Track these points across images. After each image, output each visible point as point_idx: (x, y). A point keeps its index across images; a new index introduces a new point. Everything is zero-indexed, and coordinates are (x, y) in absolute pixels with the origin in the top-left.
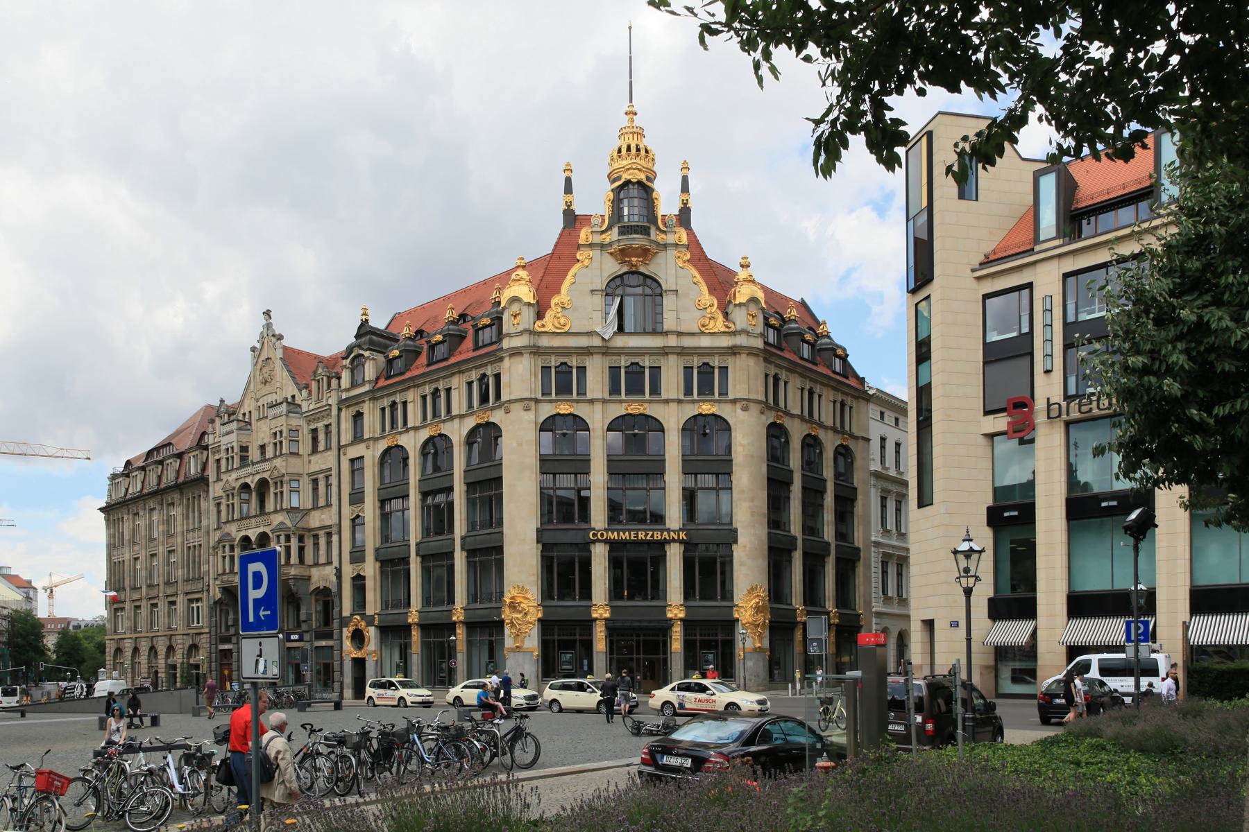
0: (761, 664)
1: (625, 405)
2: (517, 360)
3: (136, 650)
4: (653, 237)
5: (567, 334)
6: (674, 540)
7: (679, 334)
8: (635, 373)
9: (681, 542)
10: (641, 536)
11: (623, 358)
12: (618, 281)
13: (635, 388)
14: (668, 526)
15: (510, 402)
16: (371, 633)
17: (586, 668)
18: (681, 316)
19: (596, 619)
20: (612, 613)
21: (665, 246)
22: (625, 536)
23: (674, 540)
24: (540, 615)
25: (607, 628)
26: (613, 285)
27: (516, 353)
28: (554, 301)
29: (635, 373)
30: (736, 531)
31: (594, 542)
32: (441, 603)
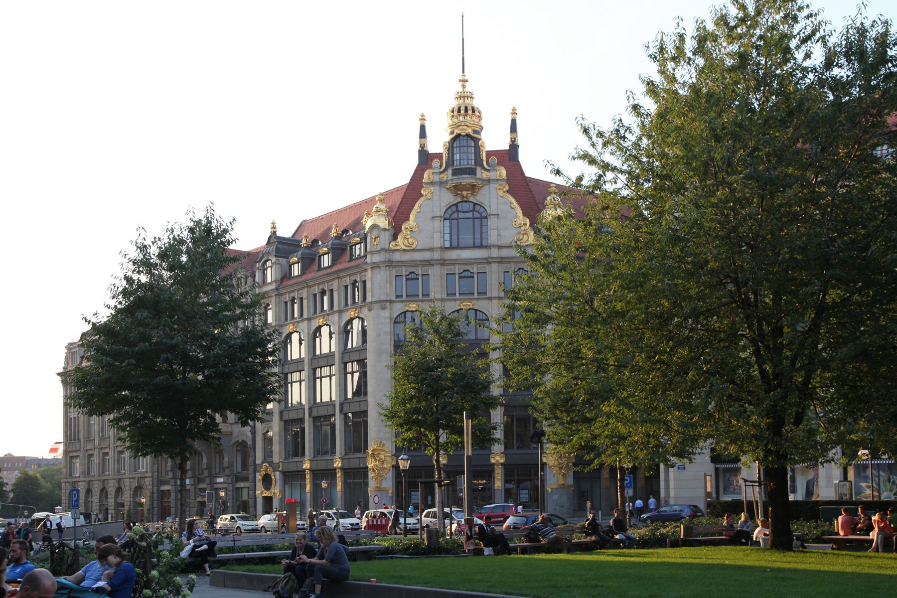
1: (458, 302)
2: (376, 271)
3: (89, 491)
4: (478, 175)
5: (414, 250)
7: (500, 247)
8: (466, 276)
11: (457, 267)
12: (454, 208)
15: (371, 303)
16: (277, 477)
17: (430, 502)
18: (502, 233)
20: (448, 461)
21: (489, 181)
26: (449, 212)
27: (375, 266)
29: (466, 276)
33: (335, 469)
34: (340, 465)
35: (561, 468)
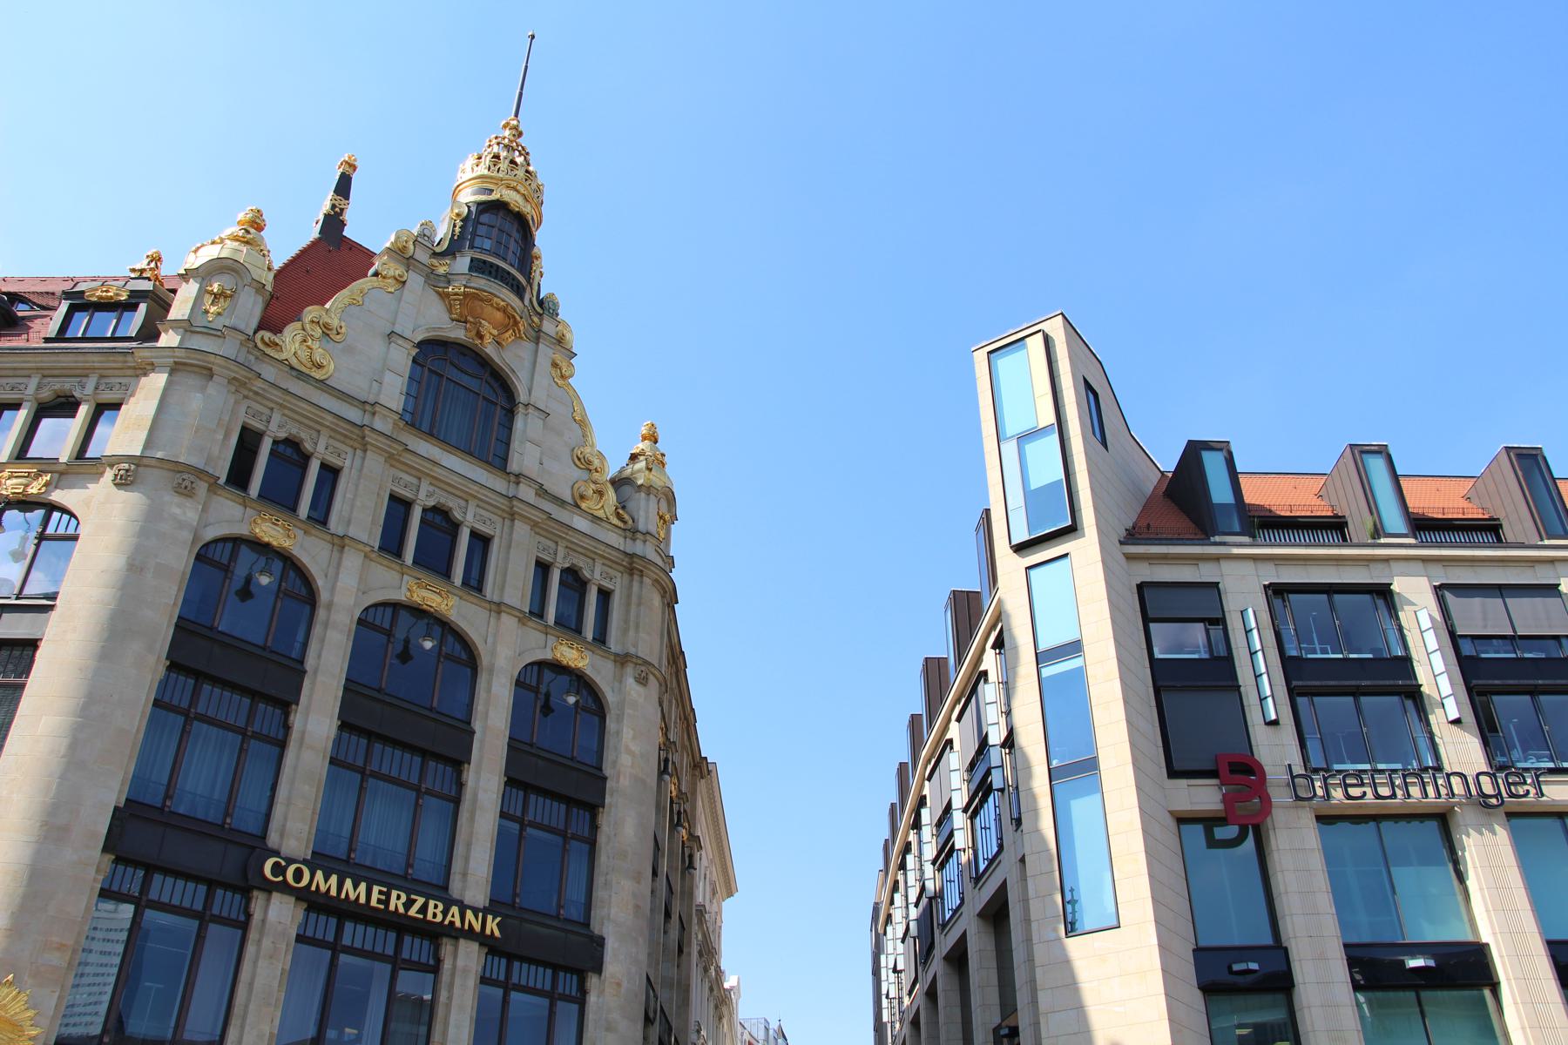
5: (322, 385)
6: (470, 934)
10: (397, 902)
13: (434, 560)
22: (354, 891)
28: (311, 312)
30: (600, 942)
31: (269, 888)
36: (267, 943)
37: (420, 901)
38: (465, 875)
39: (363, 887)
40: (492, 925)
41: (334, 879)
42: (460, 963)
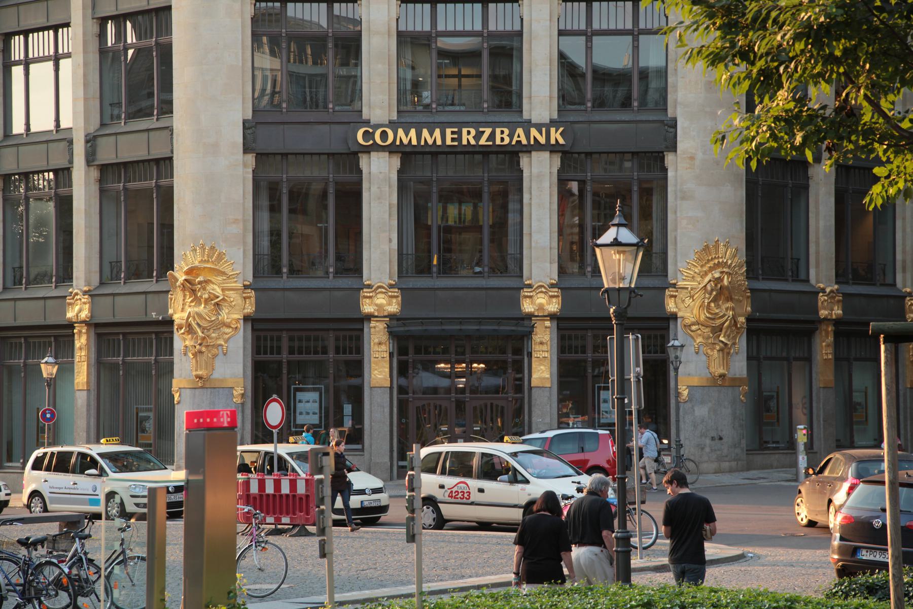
0: (727, 411)
6: (538, 146)
9: (553, 149)
10: (468, 137)
14: (526, 116)
19: (369, 317)
20: (404, 304)
23: (538, 146)
24: (250, 309)
25: (392, 334)
31: (367, 150)
32: (41, 279)
33: (70, 326)
34: (85, 315)
35: (717, 330)
36: (374, 189)
37: (488, 131)
38: (530, 97)
39: (437, 133)
40: (556, 136)
41: (413, 133)
42: (535, 171)
